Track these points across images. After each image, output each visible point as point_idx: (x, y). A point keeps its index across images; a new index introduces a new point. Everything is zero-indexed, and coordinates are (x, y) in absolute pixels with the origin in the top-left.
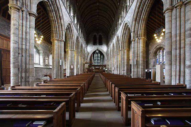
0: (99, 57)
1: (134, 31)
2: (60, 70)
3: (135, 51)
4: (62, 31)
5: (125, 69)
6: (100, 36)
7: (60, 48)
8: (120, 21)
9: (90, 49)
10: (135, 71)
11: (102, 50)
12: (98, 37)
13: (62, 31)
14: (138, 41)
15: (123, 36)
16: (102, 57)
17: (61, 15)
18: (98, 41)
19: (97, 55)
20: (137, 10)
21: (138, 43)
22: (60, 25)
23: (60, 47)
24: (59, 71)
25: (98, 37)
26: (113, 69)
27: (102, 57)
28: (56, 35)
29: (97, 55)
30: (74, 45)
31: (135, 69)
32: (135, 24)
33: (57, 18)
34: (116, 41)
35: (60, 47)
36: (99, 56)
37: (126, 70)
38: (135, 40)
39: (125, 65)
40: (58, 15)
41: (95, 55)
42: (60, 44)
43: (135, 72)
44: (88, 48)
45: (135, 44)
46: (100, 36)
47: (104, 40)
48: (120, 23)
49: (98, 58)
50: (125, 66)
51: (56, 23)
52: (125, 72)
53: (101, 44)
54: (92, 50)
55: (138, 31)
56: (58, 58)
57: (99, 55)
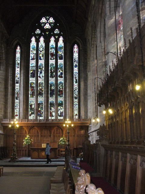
0: (61, 53)
16: (76, 55)
19: (47, 42)
27: (76, 55)
29: (47, 42)
36: (56, 48)
41: (33, 43)
49: (52, 62)
57: (61, 43)
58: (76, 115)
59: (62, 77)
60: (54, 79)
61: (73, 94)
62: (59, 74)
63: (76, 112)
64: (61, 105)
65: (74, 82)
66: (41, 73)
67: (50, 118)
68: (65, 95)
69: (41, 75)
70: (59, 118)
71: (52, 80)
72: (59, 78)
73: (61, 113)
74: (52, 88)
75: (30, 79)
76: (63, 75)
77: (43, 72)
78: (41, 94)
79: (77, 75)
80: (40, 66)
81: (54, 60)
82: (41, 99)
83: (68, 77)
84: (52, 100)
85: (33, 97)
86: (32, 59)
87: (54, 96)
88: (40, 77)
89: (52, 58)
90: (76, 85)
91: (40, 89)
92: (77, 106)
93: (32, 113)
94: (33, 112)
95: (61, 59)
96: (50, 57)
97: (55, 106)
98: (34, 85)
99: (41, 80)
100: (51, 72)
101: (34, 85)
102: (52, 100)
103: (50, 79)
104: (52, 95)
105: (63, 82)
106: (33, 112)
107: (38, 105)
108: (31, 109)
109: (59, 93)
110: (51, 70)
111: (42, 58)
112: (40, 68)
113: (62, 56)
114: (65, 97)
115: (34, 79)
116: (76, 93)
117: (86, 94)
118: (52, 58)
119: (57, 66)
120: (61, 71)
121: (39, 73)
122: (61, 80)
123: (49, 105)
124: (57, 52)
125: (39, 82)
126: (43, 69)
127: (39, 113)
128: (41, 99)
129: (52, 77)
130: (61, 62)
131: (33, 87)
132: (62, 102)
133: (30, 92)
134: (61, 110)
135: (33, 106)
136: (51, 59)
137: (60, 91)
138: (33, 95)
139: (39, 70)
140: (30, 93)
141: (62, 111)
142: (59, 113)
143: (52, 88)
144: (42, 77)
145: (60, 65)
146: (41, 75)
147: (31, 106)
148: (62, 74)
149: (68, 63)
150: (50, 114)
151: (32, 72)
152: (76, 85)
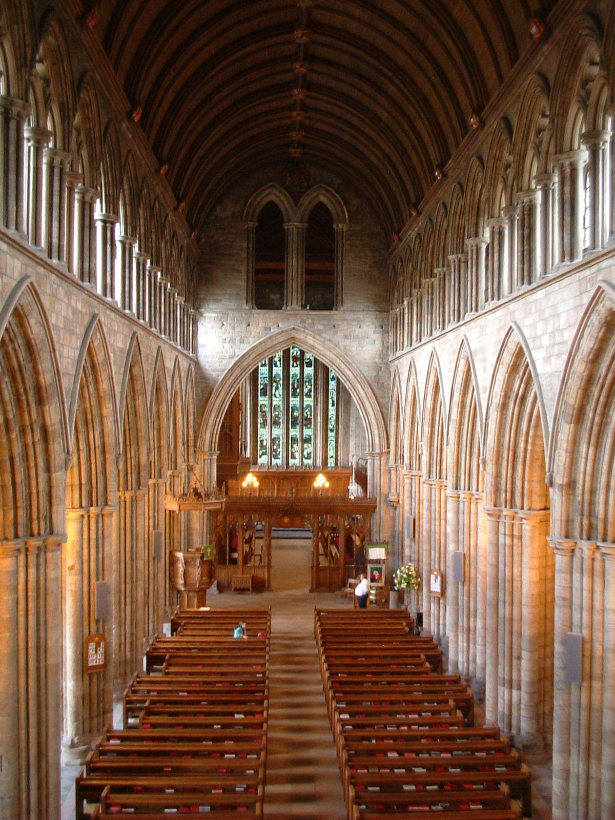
1: (571, 485)
4: (48, 469)
5: (525, 677)
7: (32, 605)
10: (573, 770)
12: (294, 226)
13: (48, 469)
14: (598, 565)
15: (504, 406)
17: (46, 378)
18: (294, 266)
20: (580, 367)
21: (597, 580)
22: (38, 436)
23: (31, 594)
24: (33, 772)
25: (294, 226)
26: (436, 587)
28: (11, 515)
30: (111, 468)
31: (574, 757)
32: (575, 442)
33: (18, 401)
35: (31, 594)
37: (531, 684)
38: (577, 553)
39: (525, 644)
40: (29, 383)
42: (32, 571)
43: (573, 780)
44: (202, 338)
45: (576, 576)
49: (295, 371)
50: (525, 654)
51: (10, 440)
52: (525, 697)
55: (593, 492)
58: (332, 457)
59: (310, 396)
60: (298, 399)
61: (327, 424)
62: (306, 390)
64: (307, 440)
65: (330, 406)
66: (277, 388)
67: (291, 461)
68: (315, 426)
69: (277, 393)
70: (306, 461)
71: (294, 402)
72: (305, 399)
73: (309, 455)
74: (296, 414)
75: (260, 398)
76: (312, 394)
77: (281, 388)
78: (275, 423)
79: (335, 393)
80: (275, 377)
81: (298, 368)
82: (278, 432)
83: (320, 398)
84: (294, 432)
85: (264, 427)
86: (262, 365)
87: (298, 427)
88: (275, 395)
89: (295, 365)
90: (332, 411)
91: (275, 415)
92: (334, 443)
93: (263, 454)
94: (264, 451)
95: (309, 365)
96: (291, 362)
97: (300, 444)
98: (267, 409)
99: (276, 401)
100: (293, 388)
101: (267, 409)
102: (294, 433)
103: (291, 399)
105: (312, 404)
106: (264, 451)
107: (273, 441)
108: (262, 447)
109: (306, 422)
110: (293, 385)
111: (278, 363)
112: (275, 382)
113: (311, 361)
114: (315, 430)
115: (267, 398)
116: (332, 424)
117: (347, 427)
118: (295, 365)
119: (303, 378)
120: (309, 387)
121: (274, 389)
122: (308, 401)
123: (290, 441)
125: (274, 403)
126: (281, 382)
127: (274, 454)
128: (278, 432)
129: (294, 395)
130: (309, 371)
131: (264, 412)
132: (310, 436)
133: (260, 420)
134: (309, 448)
135: (265, 443)
136: (293, 366)
137: (307, 419)
139: (274, 384)
140: (259, 421)
141: (309, 450)
142: (305, 453)
143: (295, 414)
144: (278, 396)
145: (308, 376)
146: (277, 393)
147: (262, 441)
148: (310, 391)
149: (320, 376)
150: (289, 455)
151: (262, 387)
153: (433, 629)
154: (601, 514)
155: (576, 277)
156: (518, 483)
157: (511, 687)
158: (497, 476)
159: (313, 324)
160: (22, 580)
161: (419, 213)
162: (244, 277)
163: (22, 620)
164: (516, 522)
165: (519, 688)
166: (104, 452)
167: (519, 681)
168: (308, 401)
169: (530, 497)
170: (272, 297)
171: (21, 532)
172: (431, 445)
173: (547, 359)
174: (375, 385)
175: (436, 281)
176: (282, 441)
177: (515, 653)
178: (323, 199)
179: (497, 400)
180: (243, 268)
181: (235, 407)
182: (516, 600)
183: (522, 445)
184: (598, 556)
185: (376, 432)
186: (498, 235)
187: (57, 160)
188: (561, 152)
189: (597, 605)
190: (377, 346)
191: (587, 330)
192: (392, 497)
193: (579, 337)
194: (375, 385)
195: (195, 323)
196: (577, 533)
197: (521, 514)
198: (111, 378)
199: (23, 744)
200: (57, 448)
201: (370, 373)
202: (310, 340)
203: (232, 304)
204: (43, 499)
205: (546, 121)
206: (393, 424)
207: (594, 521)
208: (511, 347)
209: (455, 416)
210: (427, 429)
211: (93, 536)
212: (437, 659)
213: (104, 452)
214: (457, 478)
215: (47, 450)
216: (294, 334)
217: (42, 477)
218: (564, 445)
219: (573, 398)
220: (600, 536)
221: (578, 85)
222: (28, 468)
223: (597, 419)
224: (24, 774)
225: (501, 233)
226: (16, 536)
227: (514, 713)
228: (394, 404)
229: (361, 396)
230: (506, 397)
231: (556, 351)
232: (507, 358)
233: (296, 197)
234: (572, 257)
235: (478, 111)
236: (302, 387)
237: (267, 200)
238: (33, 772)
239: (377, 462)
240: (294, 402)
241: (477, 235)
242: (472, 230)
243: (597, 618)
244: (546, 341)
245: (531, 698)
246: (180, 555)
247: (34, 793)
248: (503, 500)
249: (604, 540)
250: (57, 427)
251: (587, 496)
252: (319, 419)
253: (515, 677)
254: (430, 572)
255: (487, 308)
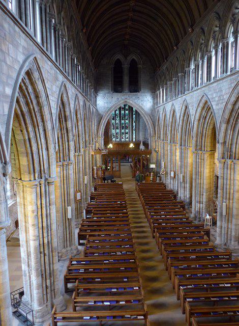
1: (225, 143)
2: (69, 229)
3: (225, 186)
6: (133, 64)
7: (65, 182)
8: (192, 67)
9: (104, 102)
10: (223, 226)
11: (140, 106)
12: (126, 66)
14: (232, 167)
15: (199, 120)
18: (126, 79)
20: (230, 107)
21: (232, 171)
24: (67, 229)
25: (126, 66)
26: (172, 175)
32: (226, 130)
34: (182, 114)
39: (204, 191)
42: (65, 171)
44: (98, 102)
45: (225, 170)
46: (133, 64)
47: (143, 78)
48: (191, 70)
49: (123, 112)
50: (204, 194)
52: (204, 206)
53: (135, 88)
54: (110, 106)
56: (63, 204)
63: (134, 137)
64: (127, 133)
67: (122, 140)
71: (123, 122)
78: (117, 128)
82: (118, 131)
83: (131, 120)
84: (123, 131)
90: (134, 124)
104: (123, 129)
107: (117, 134)
108: (113, 135)
109: (126, 128)
116: (134, 128)
117: (139, 129)
122: (127, 121)
124: (125, 107)
130: (127, 112)
134: (127, 136)
138: (114, 129)
150: (121, 138)
152: (134, 124)
153: (172, 187)
154: (234, 152)
155: (229, 78)
156: (203, 143)
157: (200, 203)
158: (197, 141)
159: (132, 97)
160: (62, 174)
161: (167, 61)
162: (110, 82)
163: (62, 186)
164: (202, 155)
165: (203, 204)
166: (79, 136)
167: (203, 202)
168: (127, 121)
169: (207, 147)
170: (119, 89)
171: (61, 160)
172: (171, 133)
173: (217, 105)
174: (151, 116)
175: (173, 82)
176: (119, 134)
177: (201, 194)
178: (134, 57)
179: (197, 118)
180: (110, 80)
181: (108, 123)
182: (202, 178)
183: (205, 132)
184: (232, 163)
185: (151, 130)
186: (197, 67)
187: (66, 45)
188: (224, 38)
189: (232, 178)
190: (152, 104)
191: (233, 95)
192: (157, 149)
193: (230, 97)
194: (151, 116)
195: (96, 97)
196: (226, 157)
197: (204, 152)
198: (80, 114)
199: (64, 222)
200: (70, 134)
201: (149, 112)
202: (131, 102)
203: (107, 92)
204: (67, 151)
205: (217, 29)
206: (157, 127)
207: (231, 153)
208: (203, 101)
209: (181, 124)
210: (170, 128)
211: (76, 162)
212: (175, 197)
213: (79, 136)
214: (181, 142)
215: (68, 135)
216: (126, 100)
217: (67, 143)
218: (223, 131)
219: (227, 116)
220: (234, 158)
221: (231, 16)
222: (63, 141)
223: (234, 122)
224: (65, 230)
225: (198, 66)
226: (60, 161)
227: (201, 210)
228: (157, 121)
229: (147, 119)
230: (200, 117)
231: (221, 102)
232: (201, 105)
233: (126, 57)
234: (226, 73)
235: (192, 26)
236: (125, 117)
237: (117, 58)
238: (67, 229)
239: (152, 139)
240: (123, 122)
241: (189, 67)
242: (188, 65)
243: (232, 182)
244: (217, 99)
245: (206, 207)
246: (95, 168)
247: (68, 235)
248: (198, 148)
249: (235, 159)
250: (70, 128)
251: (229, 146)
252: (130, 127)
253: (201, 200)
254: (171, 171)
255: (195, 89)
